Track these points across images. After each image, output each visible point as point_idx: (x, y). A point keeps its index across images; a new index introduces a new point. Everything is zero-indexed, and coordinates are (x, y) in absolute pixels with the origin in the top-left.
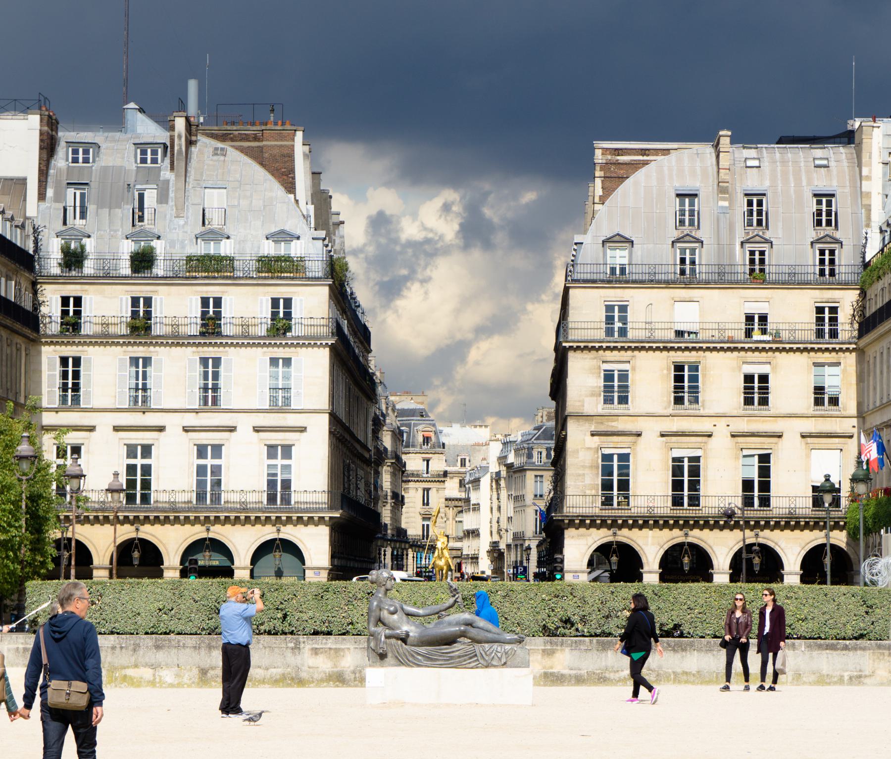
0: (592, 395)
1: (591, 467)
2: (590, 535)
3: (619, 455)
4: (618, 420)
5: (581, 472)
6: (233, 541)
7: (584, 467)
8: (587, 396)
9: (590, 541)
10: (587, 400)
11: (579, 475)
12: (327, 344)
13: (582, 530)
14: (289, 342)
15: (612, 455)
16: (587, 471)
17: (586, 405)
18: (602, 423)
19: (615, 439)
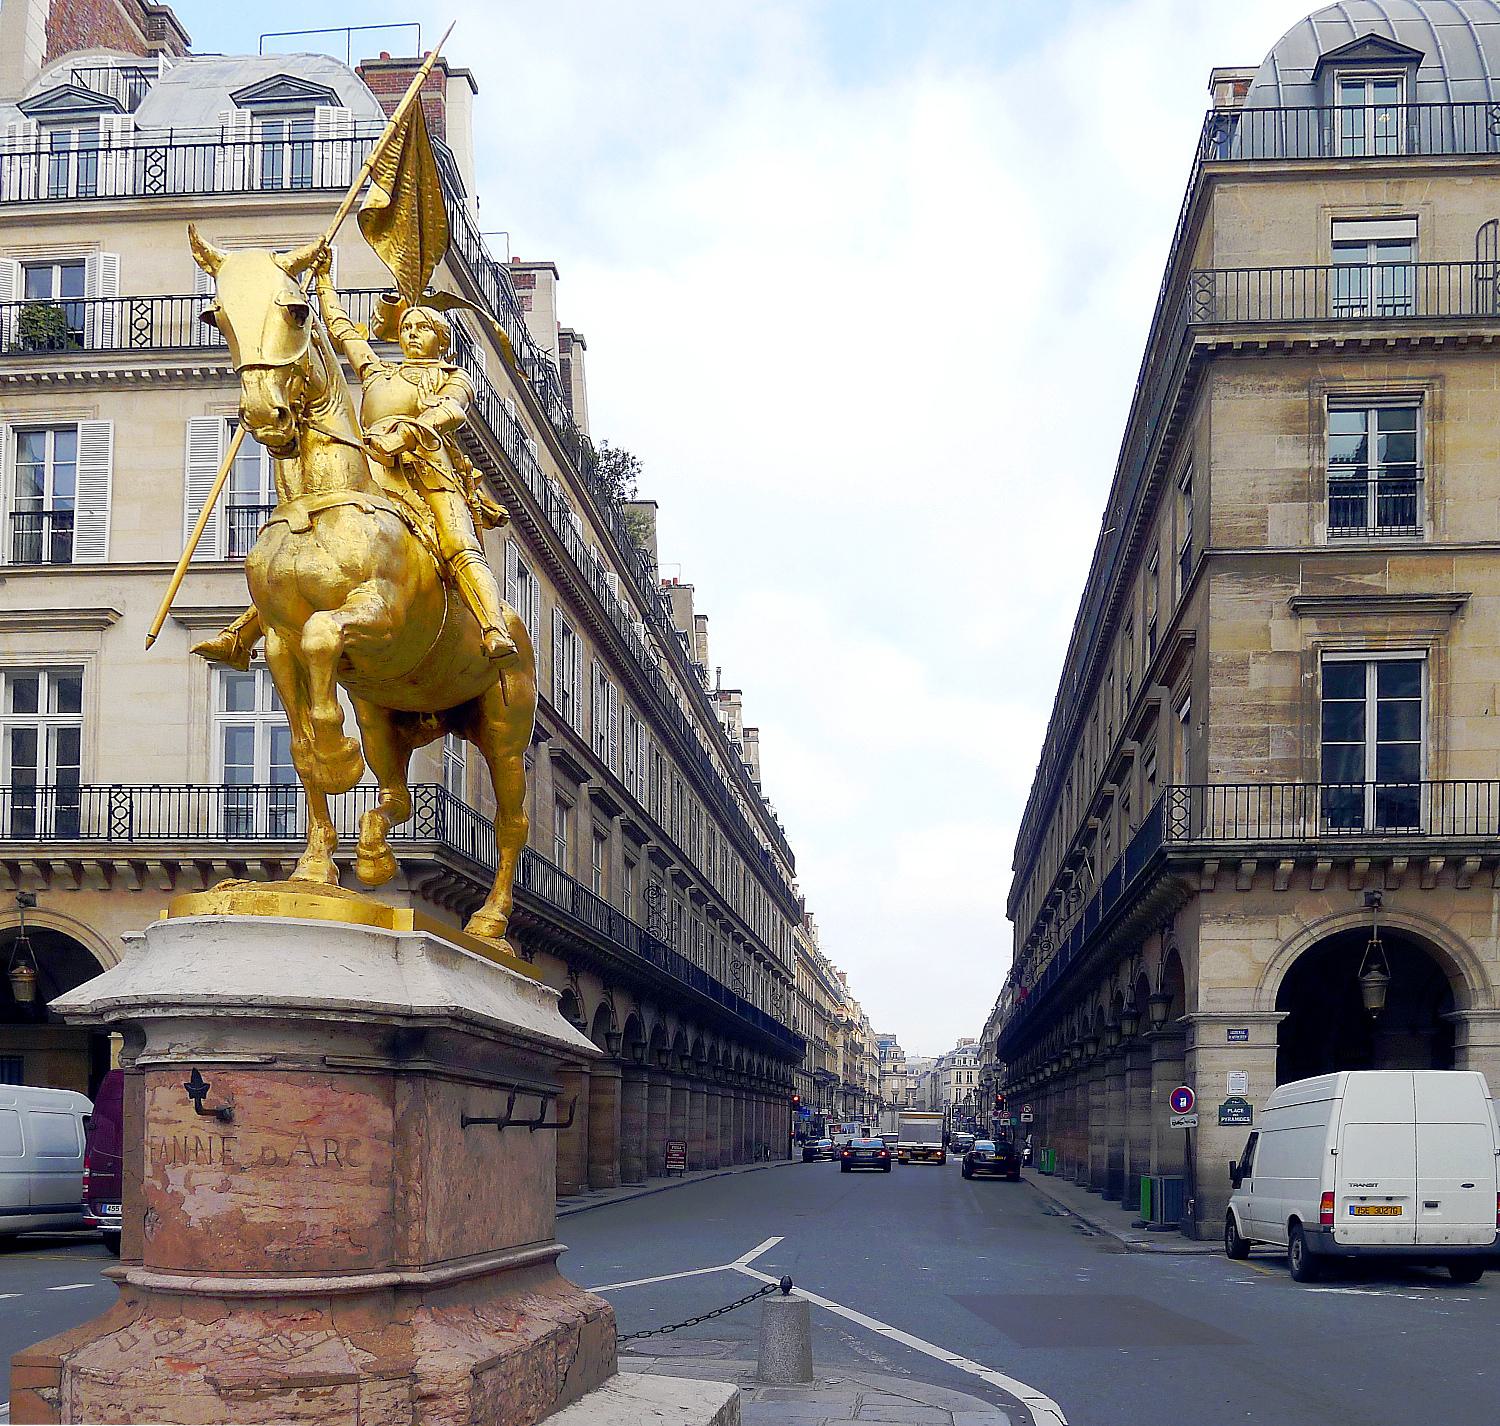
0: (1295, 496)
1: (1289, 711)
2: (1289, 911)
5: (1257, 725)
7: (1266, 710)
9: (1288, 927)
10: (1277, 511)
13: (1261, 896)
17: (1273, 525)
18: (1329, 580)
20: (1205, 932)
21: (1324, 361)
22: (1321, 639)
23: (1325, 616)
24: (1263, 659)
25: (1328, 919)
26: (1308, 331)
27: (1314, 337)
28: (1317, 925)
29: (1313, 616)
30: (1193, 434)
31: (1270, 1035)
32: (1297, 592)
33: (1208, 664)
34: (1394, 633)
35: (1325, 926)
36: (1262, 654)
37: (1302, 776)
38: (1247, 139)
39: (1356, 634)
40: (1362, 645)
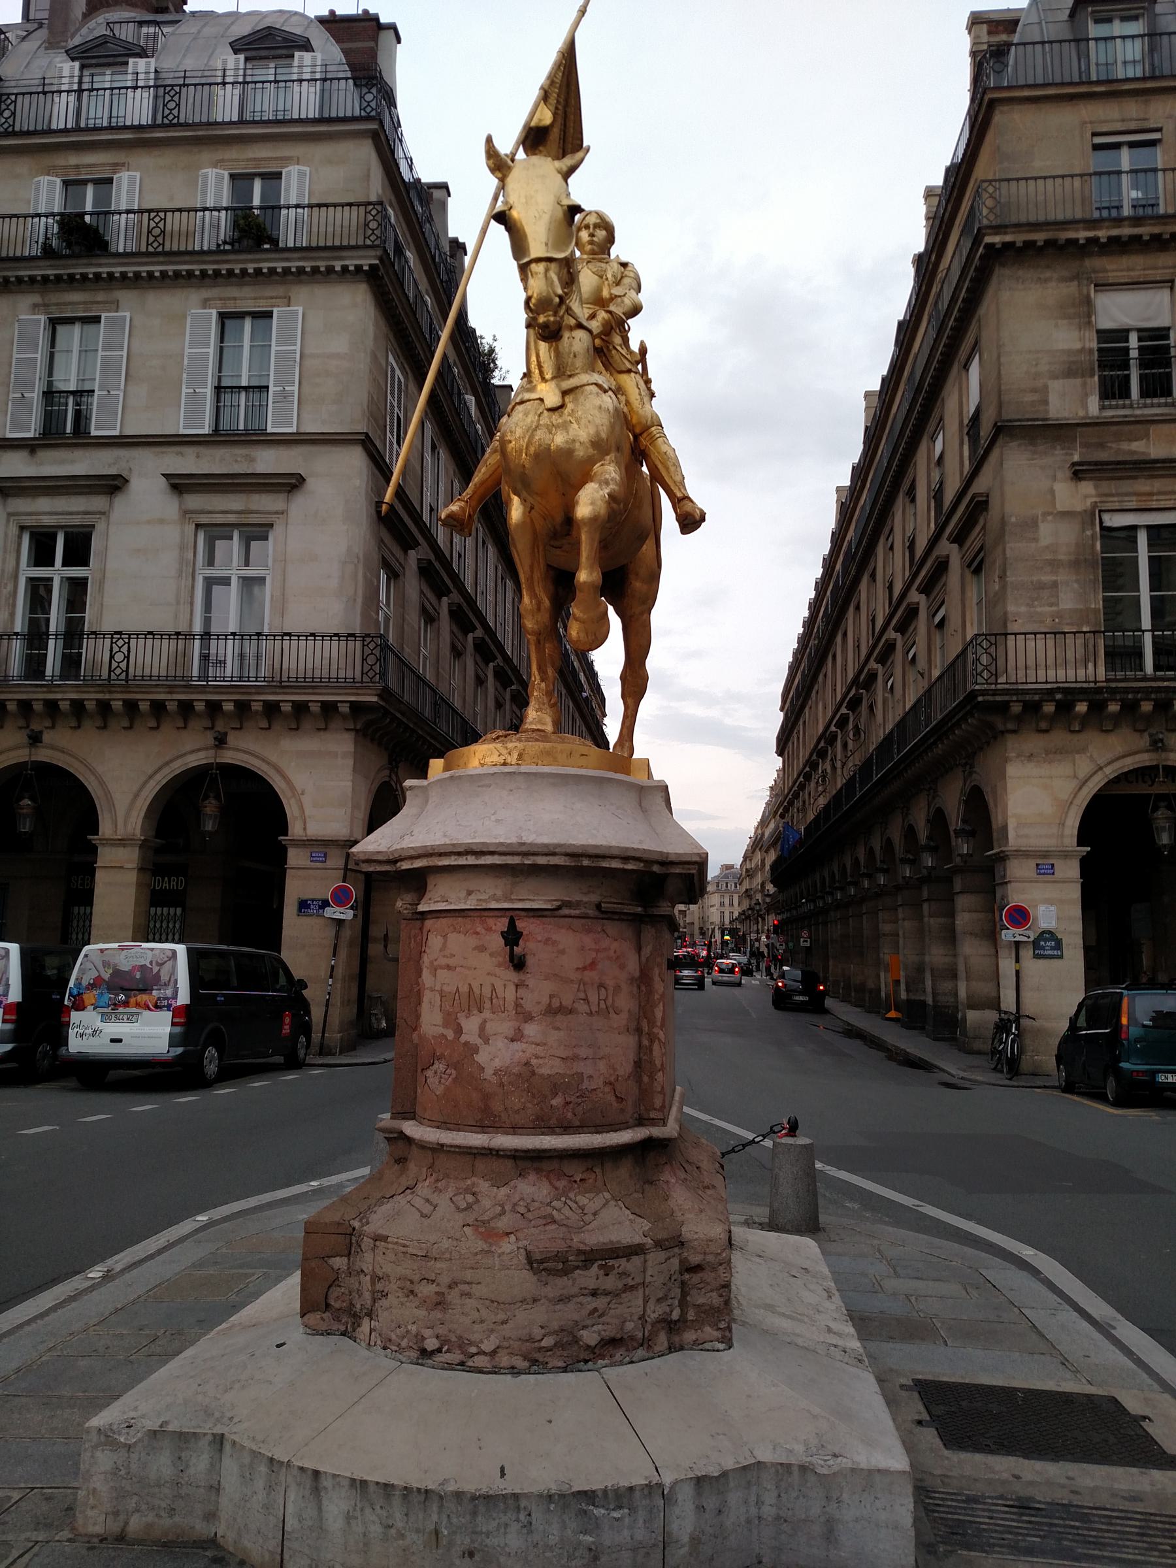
0: (1071, 371)
1: (1076, 564)
2: (1083, 750)
3: (1149, 528)
4: (1147, 436)
5: (1047, 578)
6: (100, 769)
7: (1054, 564)
8: (1057, 378)
9: (1084, 766)
10: (1056, 387)
11: (1041, 586)
12: (359, 268)
13: (1059, 737)
14: (265, 266)
15: (1134, 528)
16: (1062, 576)
18: (1101, 446)
19: (1143, 485)
20: (1012, 770)
21: (1091, 255)
22: (1097, 499)
23: (1100, 479)
24: (1050, 518)
25: (1118, 759)
26: (1077, 230)
27: (1082, 235)
28: (1109, 763)
29: (1091, 479)
30: (979, 321)
31: (1071, 870)
32: (1076, 458)
33: (1003, 521)
34: (1159, 493)
35: (1117, 765)
36: (1052, 513)
37: (1088, 623)
38: (1022, 66)
39: (1127, 494)
40: (1133, 505)
